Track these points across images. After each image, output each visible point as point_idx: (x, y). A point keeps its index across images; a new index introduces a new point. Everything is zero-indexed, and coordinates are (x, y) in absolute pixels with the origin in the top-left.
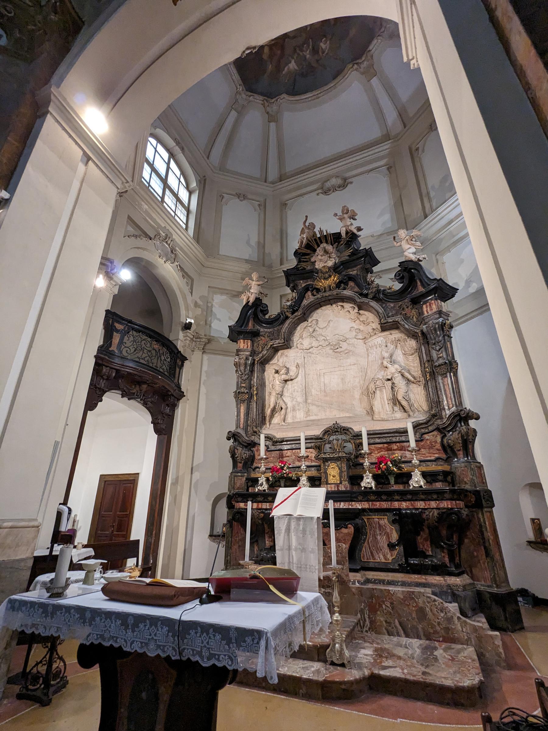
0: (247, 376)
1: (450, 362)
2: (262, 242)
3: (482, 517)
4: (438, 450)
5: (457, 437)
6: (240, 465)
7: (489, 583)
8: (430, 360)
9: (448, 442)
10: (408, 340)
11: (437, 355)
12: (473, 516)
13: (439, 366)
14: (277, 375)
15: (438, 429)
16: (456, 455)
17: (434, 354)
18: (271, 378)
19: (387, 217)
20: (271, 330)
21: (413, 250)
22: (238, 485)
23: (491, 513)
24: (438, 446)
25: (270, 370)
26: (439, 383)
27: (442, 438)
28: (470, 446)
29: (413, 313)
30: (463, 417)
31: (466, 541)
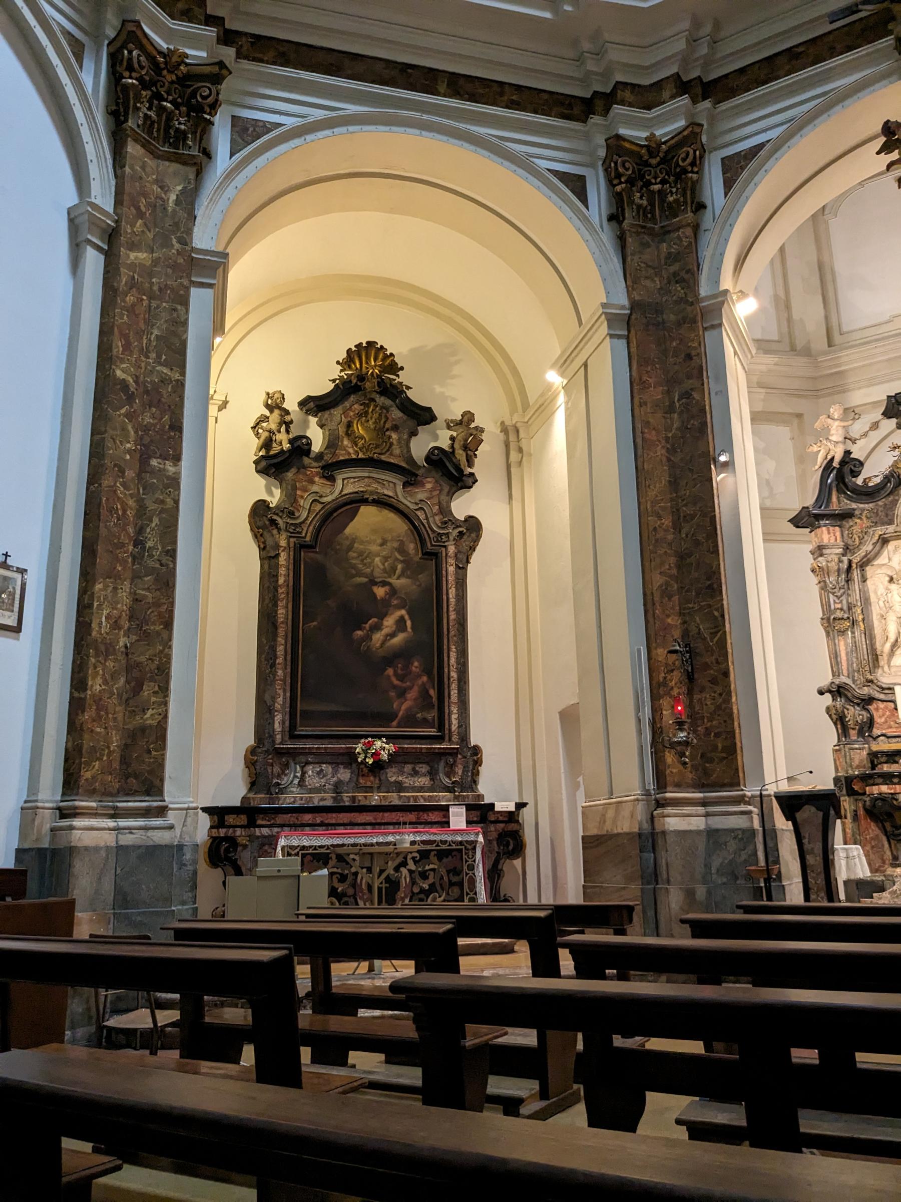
0: (842, 591)
2: (782, 294)
6: (853, 734)
14: (893, 587)
18: (881, 590)
20: (871, 505)
22: (856, 762)
25: (876, 579)
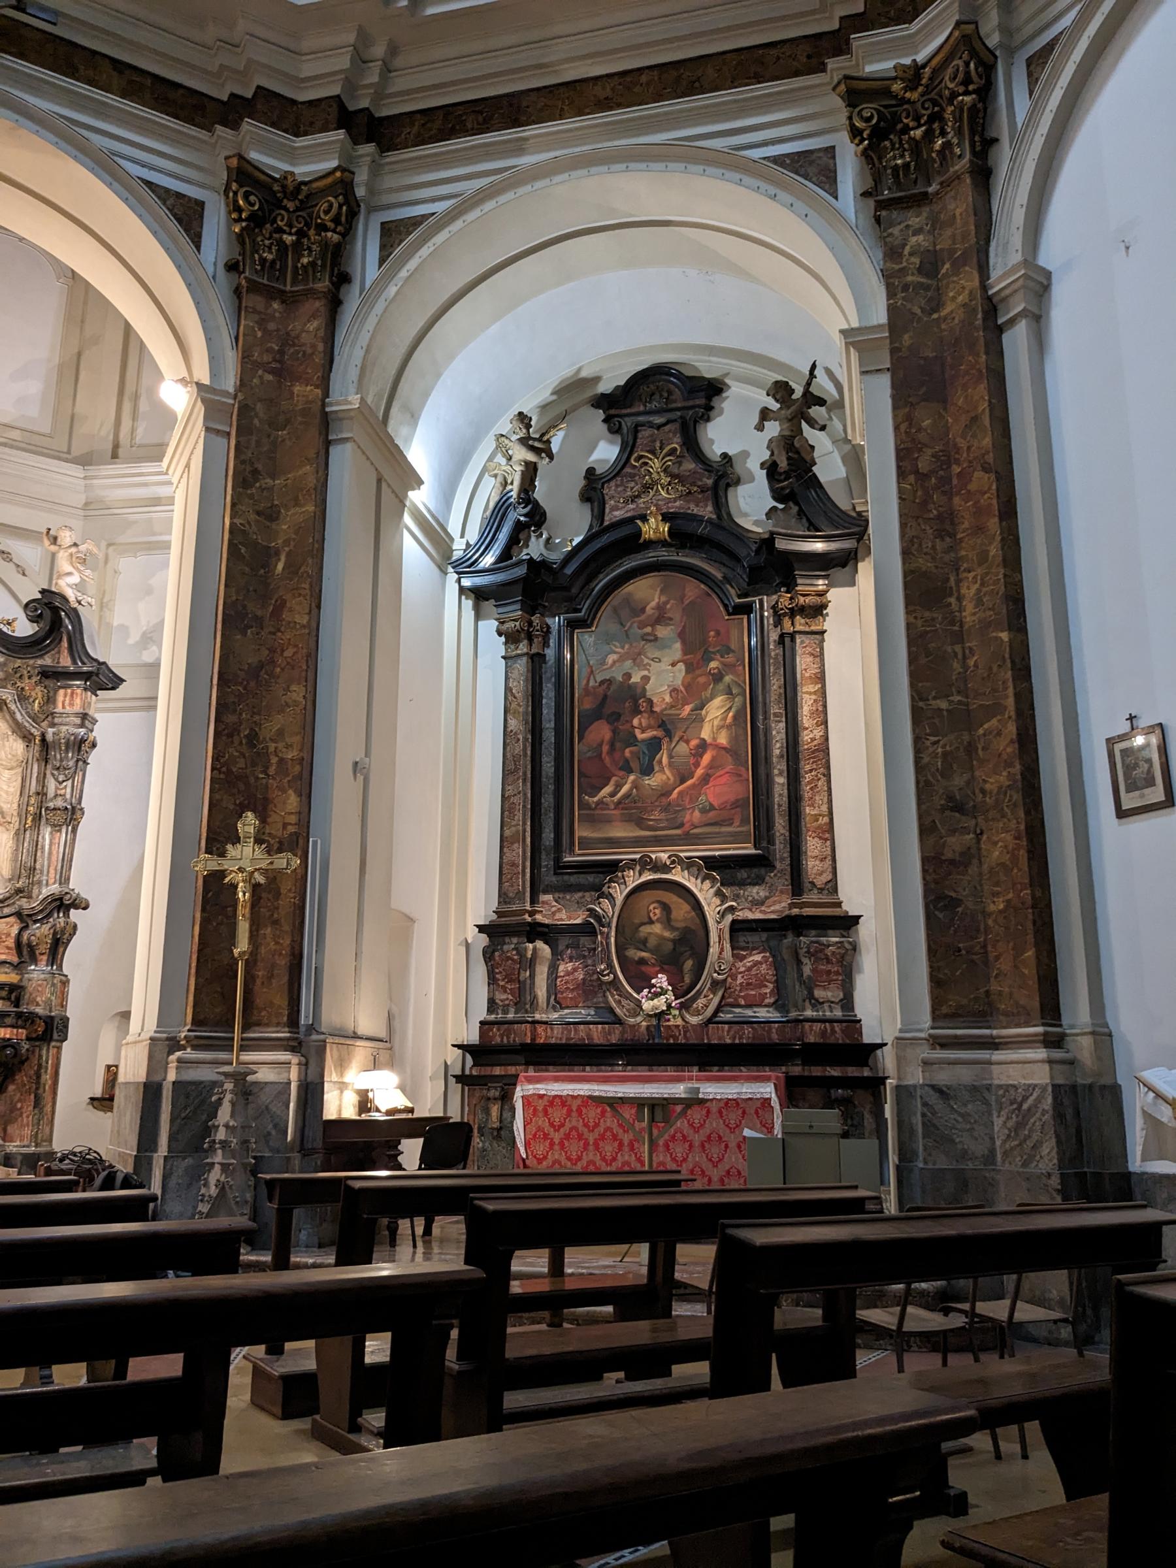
1: (73, 808)
3: (47, 1054)
4: (8, 948)
5: (46, 933)
7: (26, 1142)
8: (41, 794)
9: (29, 939)
10: (12, 738)
11: (57, 788)
12: (33, 1052)
13: (55, 809)
15: (18, 914)
16: (34, 960)
17: (51, 785)
19: (34, 387)
21: (75, 579)
23: (59, 1048)
24: (11, 942)
26: (43, 838)
27: (21, 930)
28: (61, 950)
29: (38, 694)
30: (63, 904)
31: (11, 1088)
